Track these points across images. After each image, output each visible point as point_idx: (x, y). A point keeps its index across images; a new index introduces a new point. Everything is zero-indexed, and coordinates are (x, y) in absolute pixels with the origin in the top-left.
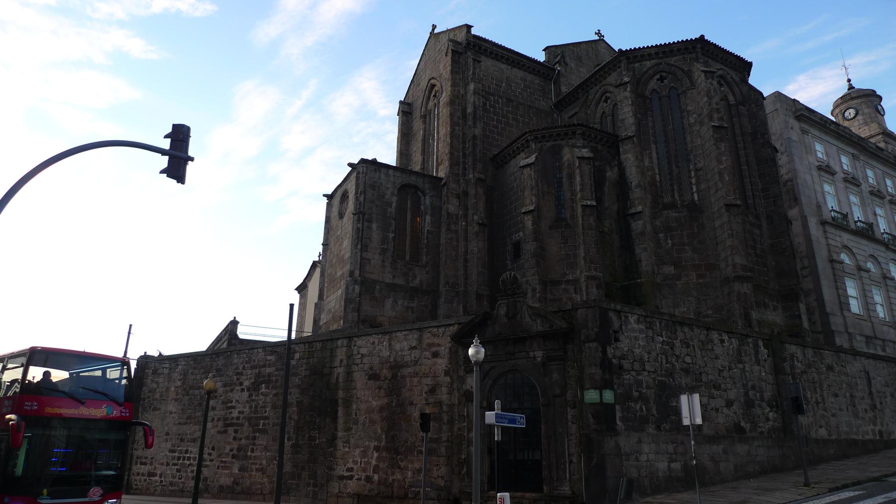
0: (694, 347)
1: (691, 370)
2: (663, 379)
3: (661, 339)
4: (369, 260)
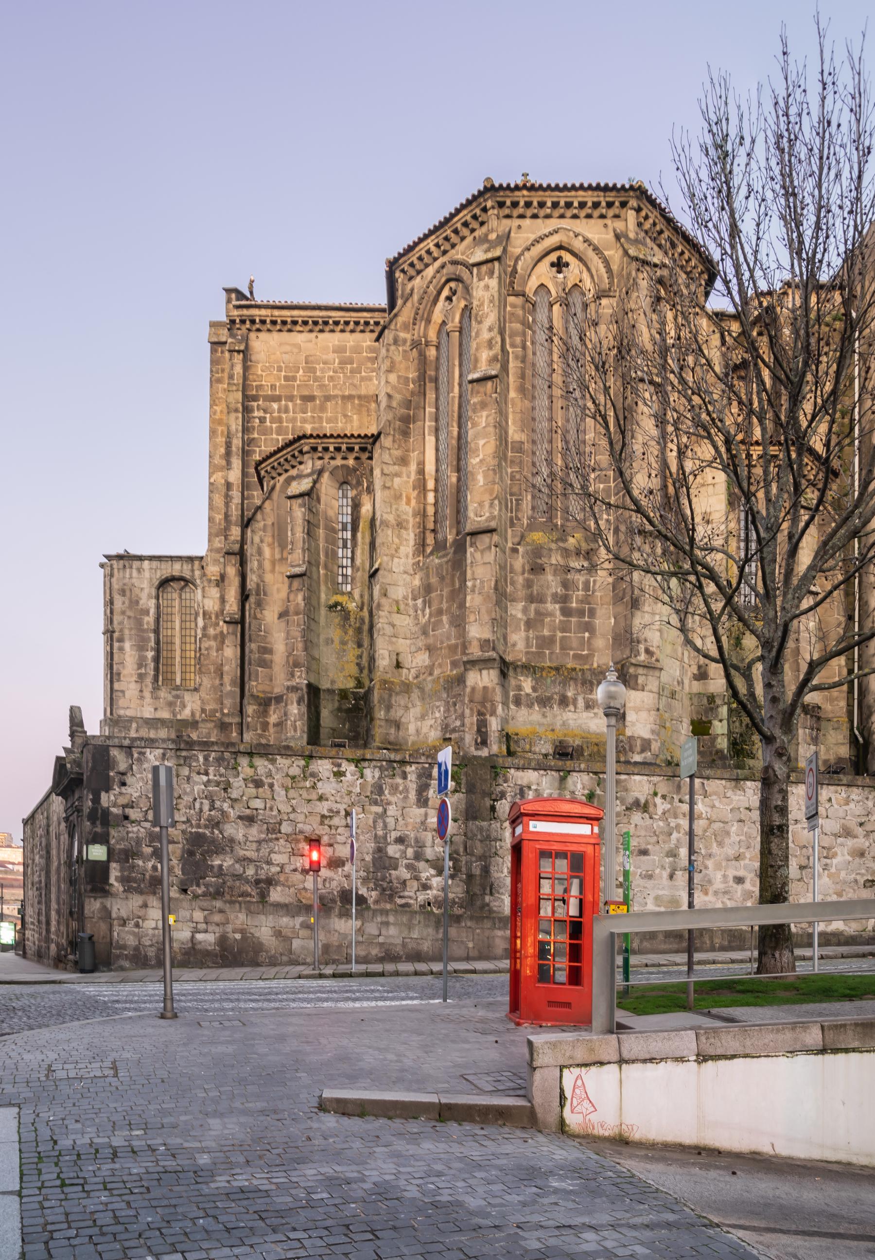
0: (271, 786)
1: (260, 817)
2: (200, 830)
3: (205, 778)
4: (123, 692)
